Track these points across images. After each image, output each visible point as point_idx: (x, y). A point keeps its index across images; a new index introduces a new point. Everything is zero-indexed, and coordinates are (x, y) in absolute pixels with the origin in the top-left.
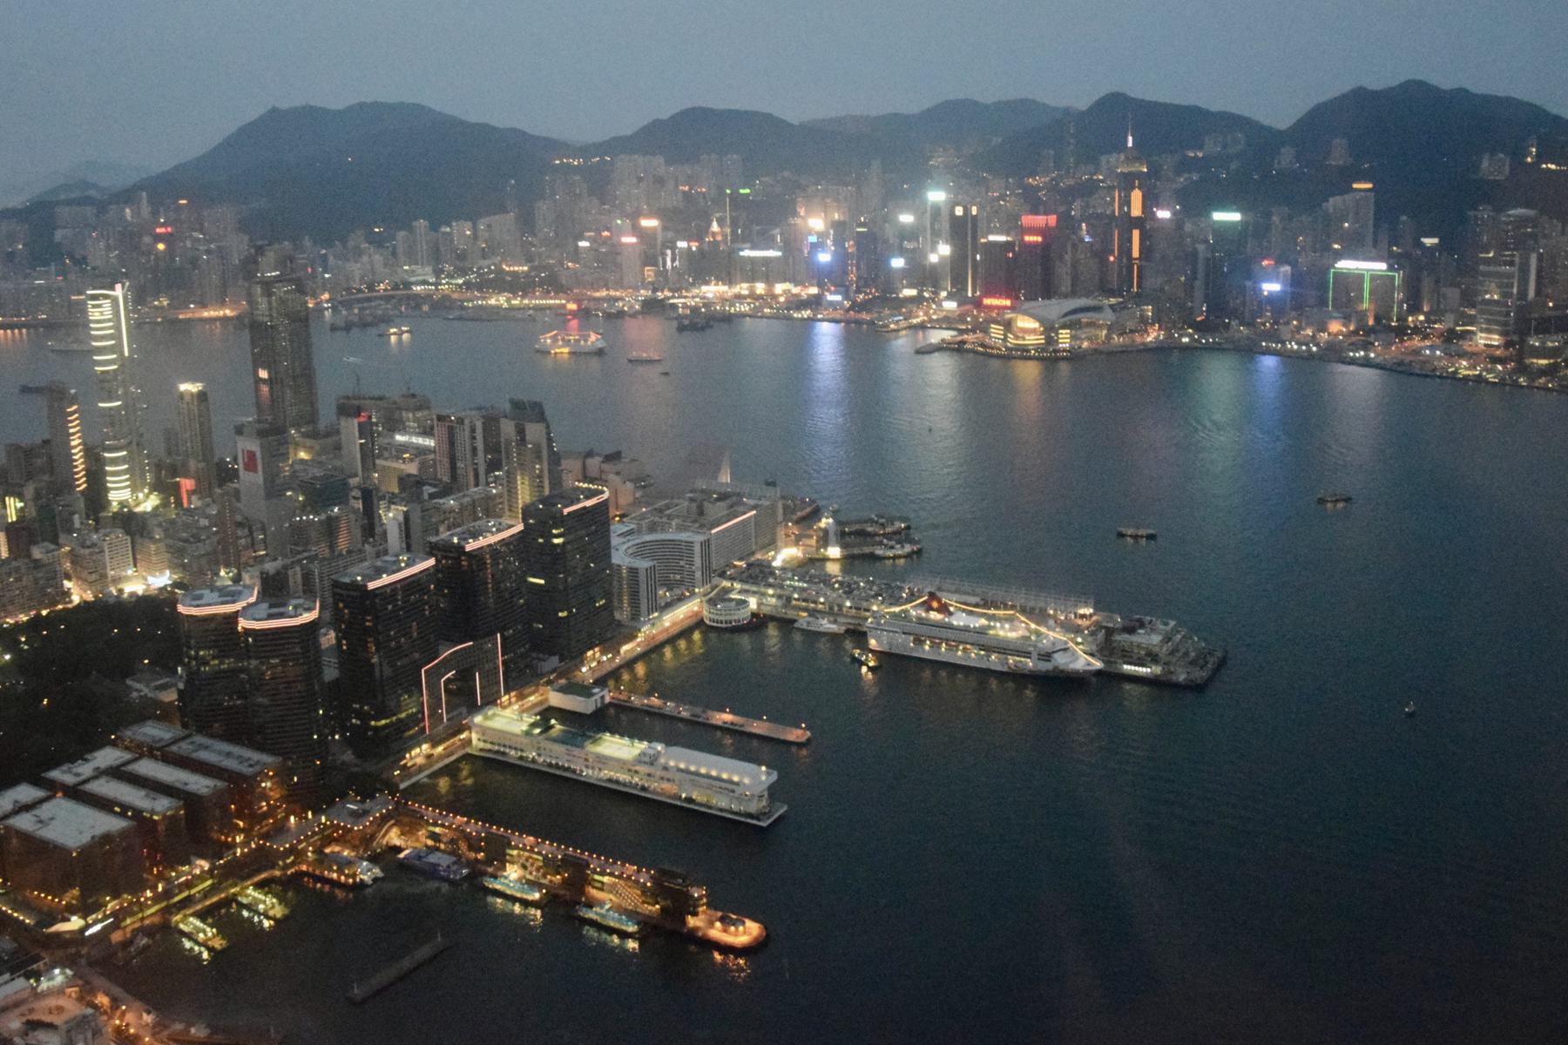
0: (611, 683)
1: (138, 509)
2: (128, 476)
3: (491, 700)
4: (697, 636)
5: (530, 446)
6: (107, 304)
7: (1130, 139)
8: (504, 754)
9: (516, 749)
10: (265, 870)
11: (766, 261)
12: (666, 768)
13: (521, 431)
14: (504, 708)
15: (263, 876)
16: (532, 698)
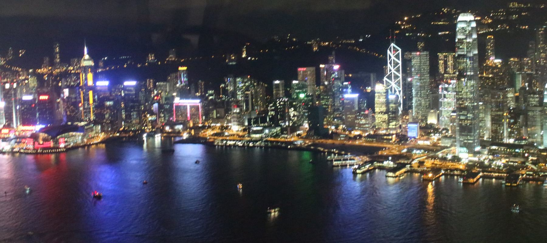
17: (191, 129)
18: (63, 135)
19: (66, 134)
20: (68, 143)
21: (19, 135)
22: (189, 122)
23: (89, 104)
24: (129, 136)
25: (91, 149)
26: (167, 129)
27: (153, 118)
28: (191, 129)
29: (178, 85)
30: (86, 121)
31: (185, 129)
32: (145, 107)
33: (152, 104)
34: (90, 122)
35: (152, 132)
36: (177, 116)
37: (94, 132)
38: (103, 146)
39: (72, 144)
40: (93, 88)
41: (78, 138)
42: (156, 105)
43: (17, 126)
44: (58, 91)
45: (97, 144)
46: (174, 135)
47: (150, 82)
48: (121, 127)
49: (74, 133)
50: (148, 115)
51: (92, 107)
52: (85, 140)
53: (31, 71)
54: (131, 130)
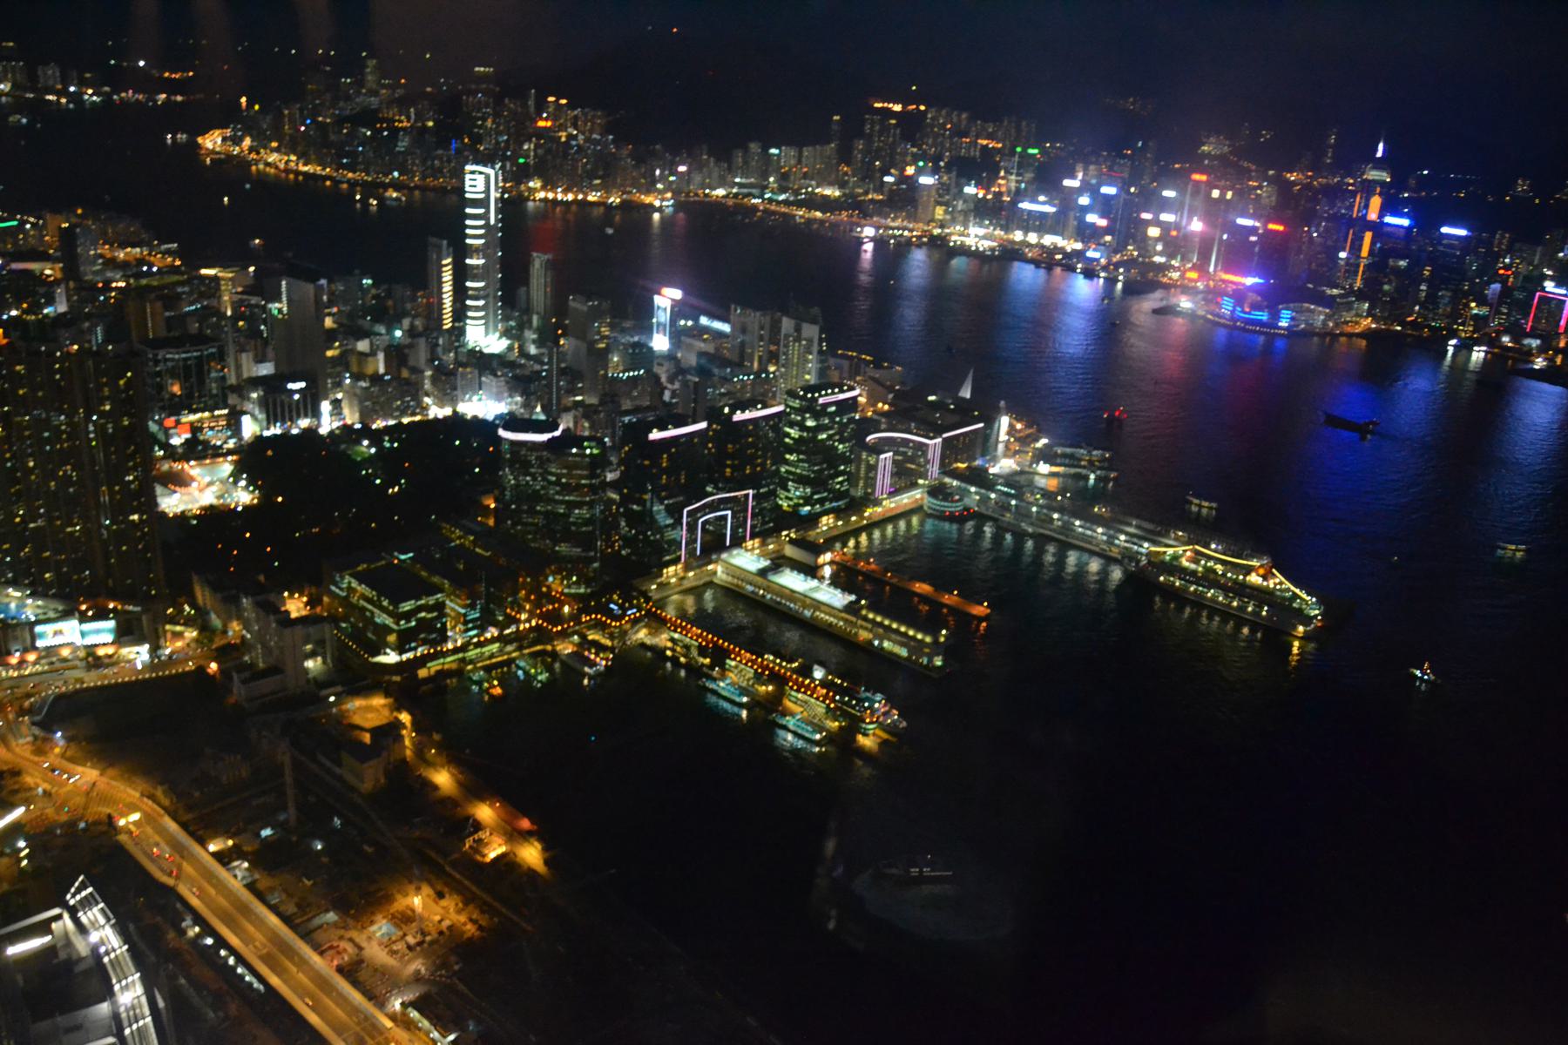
0: (838, 546)
1: (486, 351)
2: (483, 321)
3: (738, 542)
4: (915, 520)
5: (804, 342)
6: (481, 179)
7: (1381, 147)
8: (743, 588)
9: (751, 584)
10: (540, 644)
11: (1043, 215)
12: (865, 619)
13: (798, 329)
14: (747, 550)
15: (539, 648)
16: (771, 547)
17: (1558, 351)
18: (1292, 305)
19: (1296, 304)
20: (1297, 323)
21: (1215, 287)
22: (1559, 338)
23: (1359, 257)
24: (1420, 336)
25: (1336, 345)
26: (1506, 339)
27: (1484, 311)
28: (1558, 351)
29: (1561, 255)
30: (1343, 288)
31: (1542, 350)
32: (1473, 284)
33: (1488, 283)
34: (1351, 292)
35: (1471, 338)
36: (1537, 319)
37: (1354, 312)
38: (1364, 343)
39: (1303, 326)
40: (1378, 228)
41: (1319, 316)
42: (1496, 287)
43: (1215, 271)
44: (1309, 218)
45: (1350, 336)
46: (1516, 355)
47: (1503, 237)
48: (1410, 315)
49: (1312, 307)
50: (1473, 305)
51: (1363, 262)
52: (1331, 324)
53: (1271, 172)
54: (1429, 327)
